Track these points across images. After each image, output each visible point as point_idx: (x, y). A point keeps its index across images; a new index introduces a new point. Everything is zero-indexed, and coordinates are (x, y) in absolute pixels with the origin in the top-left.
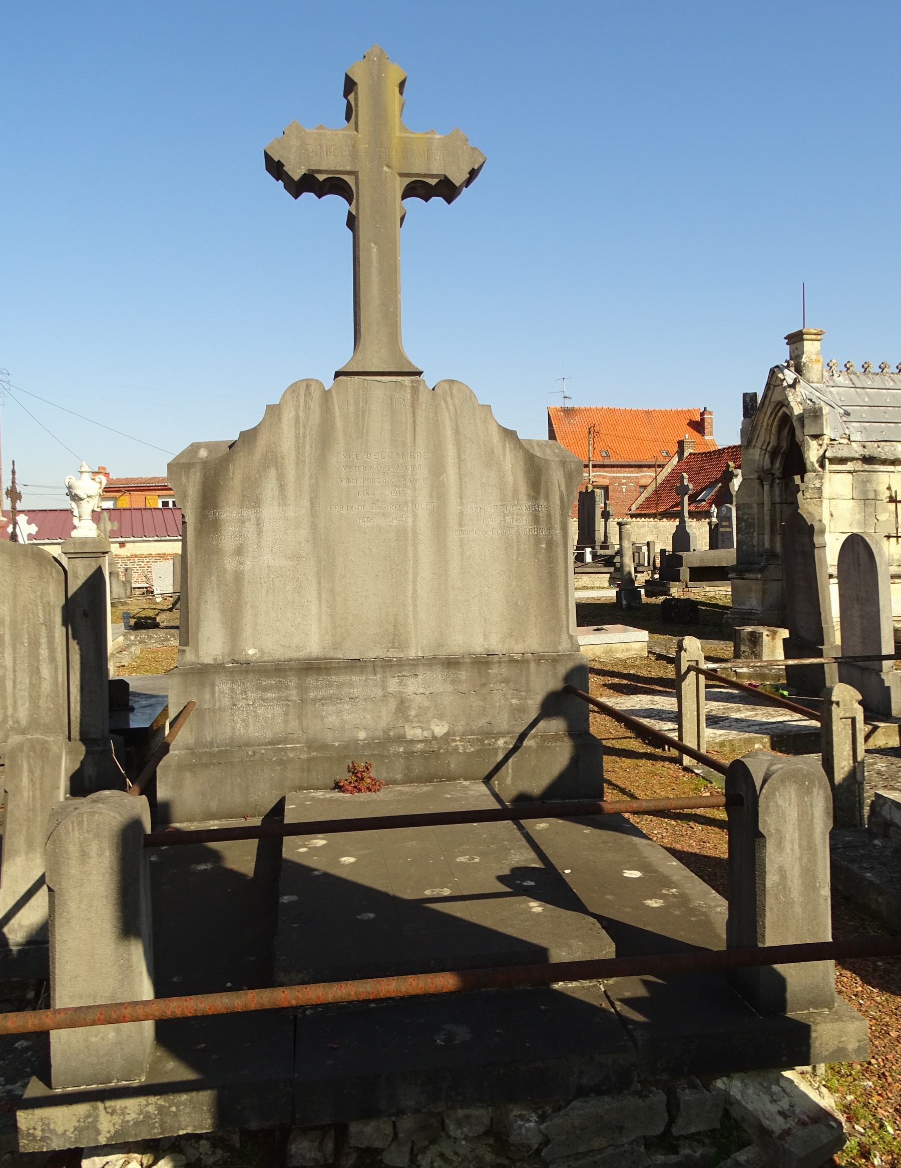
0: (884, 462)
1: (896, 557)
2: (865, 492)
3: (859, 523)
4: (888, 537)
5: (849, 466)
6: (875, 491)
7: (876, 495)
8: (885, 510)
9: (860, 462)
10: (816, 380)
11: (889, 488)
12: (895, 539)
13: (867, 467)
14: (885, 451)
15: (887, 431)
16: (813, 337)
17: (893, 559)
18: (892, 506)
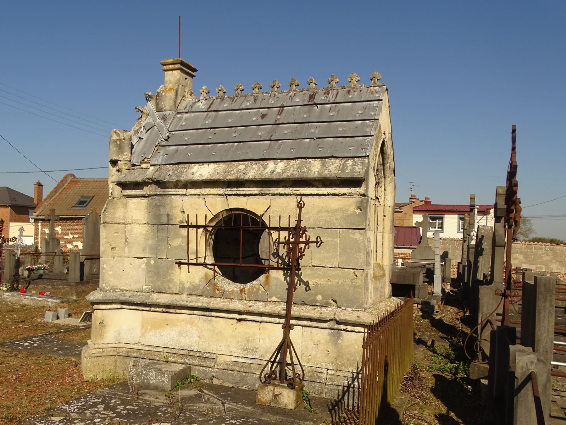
0: (177, 185)
1: (187, 285)
2: (157, 216)
3: (151, 248)
4: (179, 264)
5: (146, 190)
6: (168, 215)
7: (168, 220)
8: (178, 235)
9: (154, 186)
10: (168, 108)
11: (183, 212)
12: (186, 266)
13: (159, 191)
14: (170, 174)
15: (184, 153)
16: (171, 66)
17: (183, 288)
18: (184, 231)
